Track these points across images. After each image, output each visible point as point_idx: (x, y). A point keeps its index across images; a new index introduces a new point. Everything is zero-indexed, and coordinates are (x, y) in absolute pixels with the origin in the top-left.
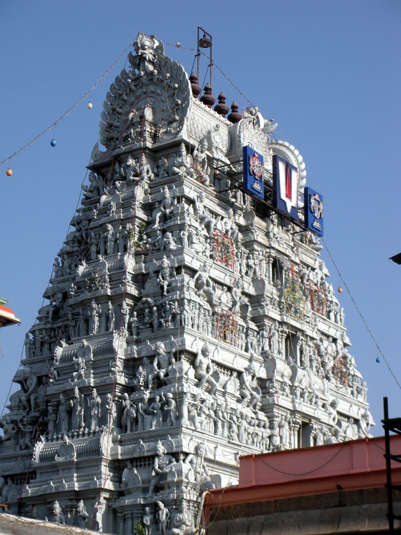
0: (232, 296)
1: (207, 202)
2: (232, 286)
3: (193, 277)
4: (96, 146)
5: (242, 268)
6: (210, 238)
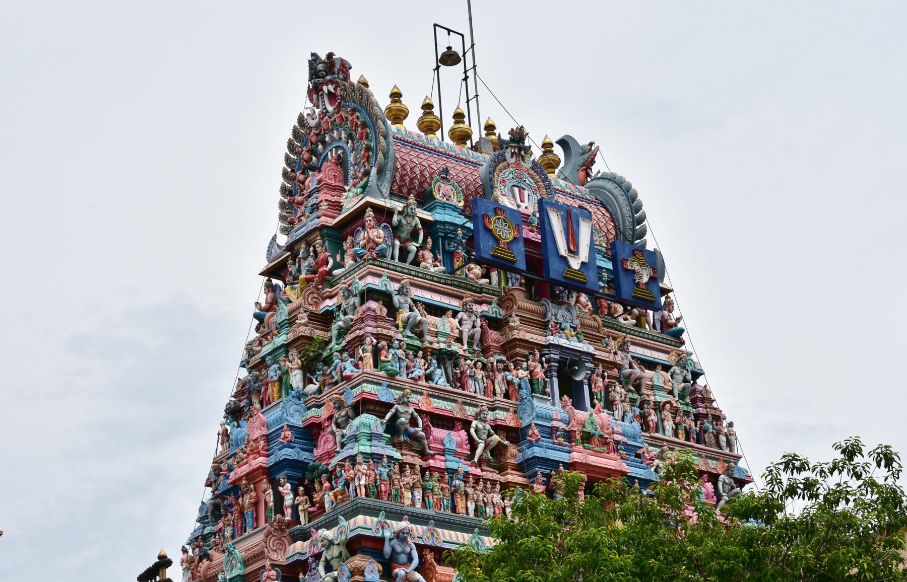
0: (469, 434)
1: (416, 293)
2: (470, 419)
3: (383, 418)
4: (274, 238)
5: (497, 387)
6: (425, 350)
